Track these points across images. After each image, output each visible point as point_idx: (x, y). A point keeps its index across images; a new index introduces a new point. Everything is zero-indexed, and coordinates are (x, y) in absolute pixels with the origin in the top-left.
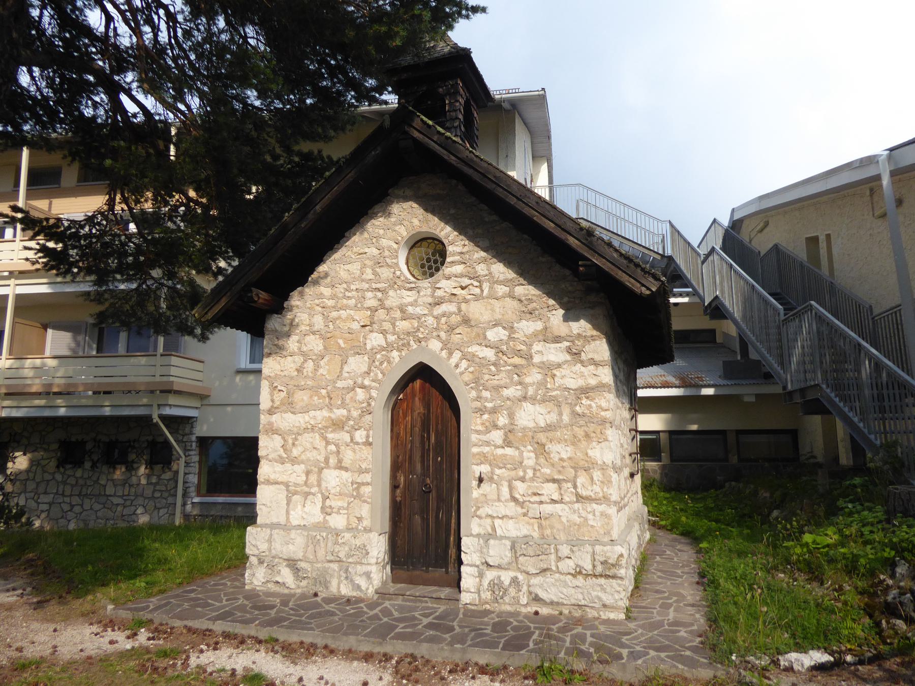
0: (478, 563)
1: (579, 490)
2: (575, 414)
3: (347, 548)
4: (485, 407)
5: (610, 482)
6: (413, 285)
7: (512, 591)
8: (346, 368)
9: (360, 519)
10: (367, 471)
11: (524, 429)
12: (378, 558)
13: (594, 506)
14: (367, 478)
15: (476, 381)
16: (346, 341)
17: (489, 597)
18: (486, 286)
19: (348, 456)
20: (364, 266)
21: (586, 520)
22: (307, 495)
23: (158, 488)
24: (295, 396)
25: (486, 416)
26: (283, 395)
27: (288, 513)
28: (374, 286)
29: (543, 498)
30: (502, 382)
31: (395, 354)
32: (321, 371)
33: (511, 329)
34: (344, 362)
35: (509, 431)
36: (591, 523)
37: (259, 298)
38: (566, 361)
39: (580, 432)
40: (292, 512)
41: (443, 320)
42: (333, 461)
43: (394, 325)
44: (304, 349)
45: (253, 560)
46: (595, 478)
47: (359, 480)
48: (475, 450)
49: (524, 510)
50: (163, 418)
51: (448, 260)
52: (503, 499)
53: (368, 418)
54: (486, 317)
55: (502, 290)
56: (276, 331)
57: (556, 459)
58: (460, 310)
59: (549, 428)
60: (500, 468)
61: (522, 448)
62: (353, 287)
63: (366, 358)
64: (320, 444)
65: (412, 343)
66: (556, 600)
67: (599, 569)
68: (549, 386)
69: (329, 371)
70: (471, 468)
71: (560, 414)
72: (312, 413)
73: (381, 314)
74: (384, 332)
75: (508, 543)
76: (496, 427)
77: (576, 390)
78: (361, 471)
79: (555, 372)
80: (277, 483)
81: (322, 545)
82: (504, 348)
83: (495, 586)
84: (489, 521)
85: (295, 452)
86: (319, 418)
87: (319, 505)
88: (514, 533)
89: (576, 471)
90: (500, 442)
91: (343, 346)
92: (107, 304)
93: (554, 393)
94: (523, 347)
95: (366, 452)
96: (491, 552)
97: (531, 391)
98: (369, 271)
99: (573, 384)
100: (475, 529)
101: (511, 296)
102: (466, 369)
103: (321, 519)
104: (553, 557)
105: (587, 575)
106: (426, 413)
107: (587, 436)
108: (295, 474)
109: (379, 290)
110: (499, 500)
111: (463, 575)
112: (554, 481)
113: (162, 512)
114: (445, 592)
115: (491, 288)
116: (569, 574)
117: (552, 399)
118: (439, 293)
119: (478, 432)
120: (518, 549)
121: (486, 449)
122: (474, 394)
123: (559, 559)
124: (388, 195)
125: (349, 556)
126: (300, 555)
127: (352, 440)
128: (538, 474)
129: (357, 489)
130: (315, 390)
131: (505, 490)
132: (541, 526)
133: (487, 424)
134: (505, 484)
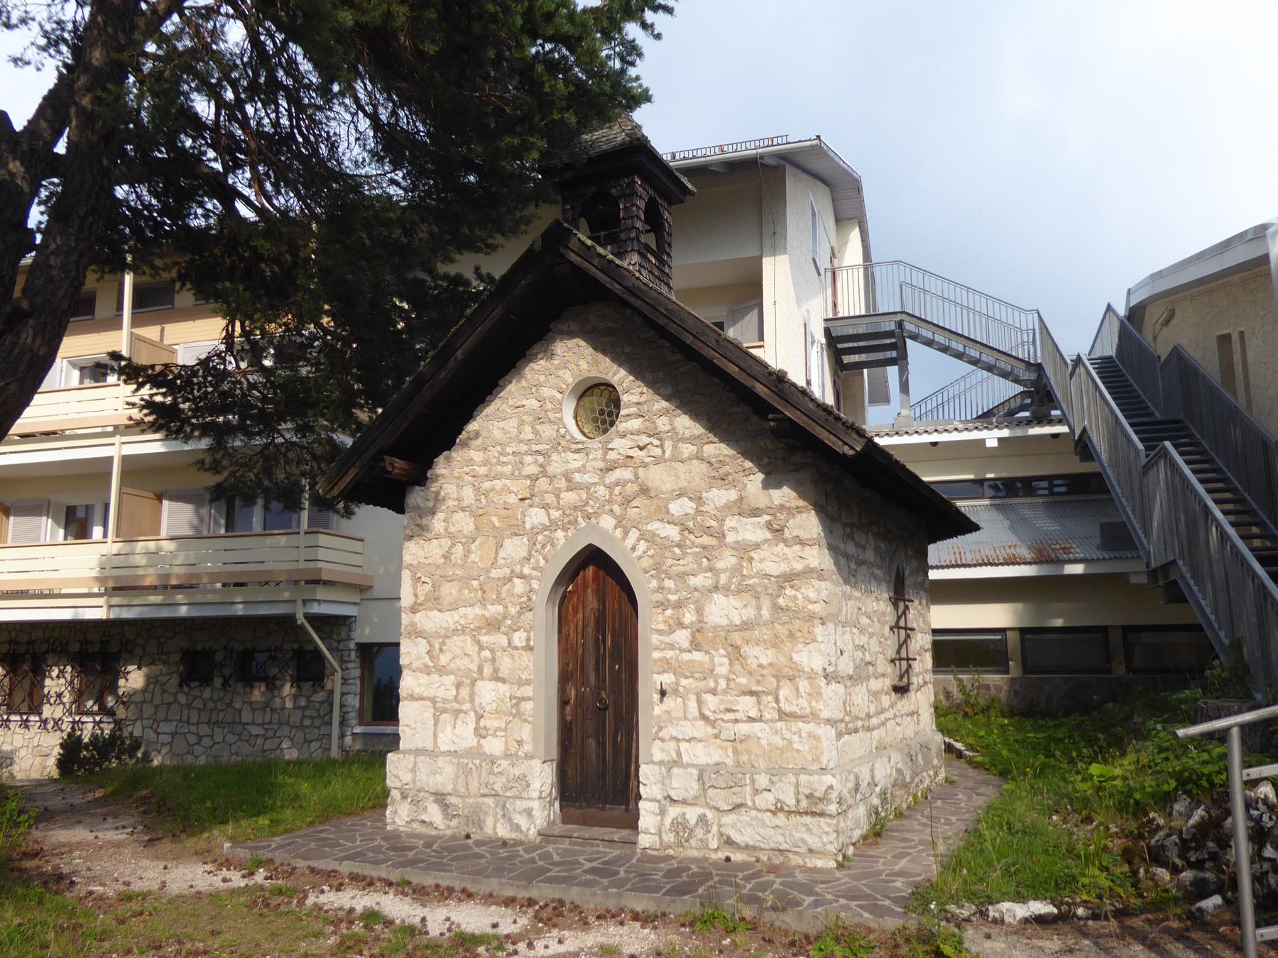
0: (659, 797)
1: (782, 705)
2: (776, 608)
3: (504, 779)
5: (819, 694)
6: (580, 446)
7: (699, 832)
8: (502, 554)
9: (520, 743)
10: (528, 683)
13: (800, 724)
14: (528, 691)
15: (657, 567)
16: (501, 518)
17: (672, 840)
18: (668, 445)
19: (506, 664)
20: (522, 423)
21: (790, 742)
22: (457, 713)
23: (308, 713)
24: (443, 589)
25: (669, 612)
26: (428, 587)
27: (435, 736)
28: (534, 448)
29: (739, 716)
30: (688, 569)
31: (560, 534)
32: (472, 557)
33: (699, 500)
34: (500, 546)
36: (796, 746)
38: (766, 540)
39: (782, 631)
40: (440, 735)
41: (617, 490)
42: (487, 670)
43: (558, 497)
44: (452, 529)
45: (395, 794)
46: (801, 690)
47: (518, 694)
48: (656, 655)
49: (716, 731)
50: (311, 618)
51: (623, 412)
52: (690, 717)
53: (529, 615)
55: (687, 449)
56: (419, 507)
57: (754, 666)
58: (637, 477)
59: (746, 626)
60: (687, 677)
61: (713, 652)
62: (509, 450)
63: (525, 540)
64: (471, 649)
65: (580, 519)
66: (751, 843)
67: (804, 804)
68: (745, 572)
69: (481, 557)
70: (650, 679)
71: (759, 608)
72: (462, 610)
73: (543, 483)
74: (546, 507)
75: (695, 772)
76: (681, 625)
78: (521, 683)
79: (752, 554)
80: (422, 699)
81: (475, 775)
82: (691, 524)
83: (680, 826)
84: (673, 744)
85: (443, 660)
86: (471, 617)
87: (472, 725)
88: (703, 760)
89: (778, 681)
90: (686, 645)
91: (497, 525)
92: (225, 474)
93: (751, 582)
94: (714, 523)
95: (526, 659)
96: (675, 784)
97: (723, 579)
98: (528, 429)
99: (774, 569)
100: (658, 755)
102: (645, 552)
103: (475, 743)
104: (748, 789)
105: (790, 812)
107: (791, 635)
108: (443, 687)
110: (686, 718)
111: (642, 812)
112: (752, 693)
113: (315, 745)
114: (617, 834)
115: (675, 447)
117: (749, 589)
118: (612, 455)
119: (660, 632)
120: (706, 778)
122: (654, 583)
123: (757, 792)
125: (506, 789)
129: (517, 705)
130: (465, 581)
131: (693, 705)
132: (735, 751)
133: (671, 622)
134: (693, 697)
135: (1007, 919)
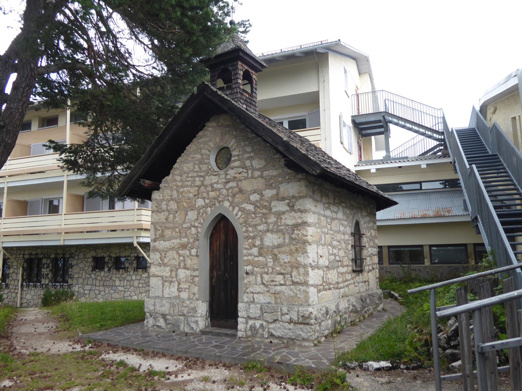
0: (246, 316)
1: (293, 279)
2: (291, 239)
3: (187, 309)
4: (250, 236)
5: (308, 274)
6: (216, 173)
7: (260, 331)
8: (187, 218)
9: (194, 294)
10: (197, 270)
11: (268, 247)
12: (202, 314)
13: (300, 287)
14: (196, 273)
15: (245, 222)
16: (187, 203)
17: (250, 334)
18: (250, 172)
19: (189, 262)
20: (195, 164)
21: (296, 294)
22: (171, 282)
23: (141, 282)
24: (165, 232)
25: (250, 240)
26: (160, 232)
27: (163, 291)
28: (199, 174)
29: (277, 283)
30: (257, 223)
31: (209, 209)
32: (177, 219)
33: (262, 195)
34: (186, 214)
35: (261, 248)
36: (299, 296)
37: (145, 184)
38: (287, 211)
39: (293, 248)
40: (165, 291)
41: (230, 191)
42: (182, 265)
43: (208, 194)
44: (169, 208)
45: (148, 315)
46: (301, 272)
47: (193, 274)
48: (245, 258)
49: (268, 289)
50: (139, 243)
51: (233, 159)
52: (258, 284)
53: (197, 243)
54: (249, 189)
55: (257, 173)
56: (157, 199)
57: (283, 263)
58: (238, 185)
59: (279, 246)
60: (257, 267)
61: (267, 257)
62: (190, 175)
63: (196, 212)
64: (176, 256)
65: (216, 203)
66: (280, 335)
67: (301, 320)
68: (279, 224)
69: (179, 220)
70: (243, 268)
71: (284, 239)
72: (172, 241)
73: (202, 189)
74: (204, 198)
75: (259, 306)
76: (255, 246)
77: (291, 226)
78: (195, 270)
79: (282, 216)
80: (158, 276)
81: (177, 307)
82: (258, 204)
83: (253, 328)
84: (251, 295)
85: (166, 261)
86: (176, 243)
87: (176, 287)
88: (263, 301)
89: (292, 269)
90: (256, 254)
91: (185, 206)
92: (93, 187)
93: (282, 228)
94: (267, 204)
95: (196, 260)
96: (251, 311)
97: (271, 227)
98: (197, 166)
99: (290, 222)
100: (246, 300)
101: (261, 176)
102: (241, 216)
103: (177, 294)
104: (279, 313)
105: (295, 323)
106: (223, 240)
107: (297, 250)
108: (166, 272)
109: (201, 176)
110: (256, 284)
111: (239, 322)
112: (282, 274)
113: (144, 295)
114: (229, 332)
115: (252, 173)
116: (287, 322)
117: (281, 231)
118: (228, 177)
119: (246, 249)
120: (263, 309)
121: (250, 258)
122: (244, 229)
123: (283, 315)
124: (205, 126)
125: (188, 313)
126: (167, 312)
127: (190, 254)
128: (274, 270)
129: (193, 279)
130: (173, 229)
131: (259, 279)
132: (275, 298)
133: (251, 245)
134: (259, 275)
135: (370, 369)
